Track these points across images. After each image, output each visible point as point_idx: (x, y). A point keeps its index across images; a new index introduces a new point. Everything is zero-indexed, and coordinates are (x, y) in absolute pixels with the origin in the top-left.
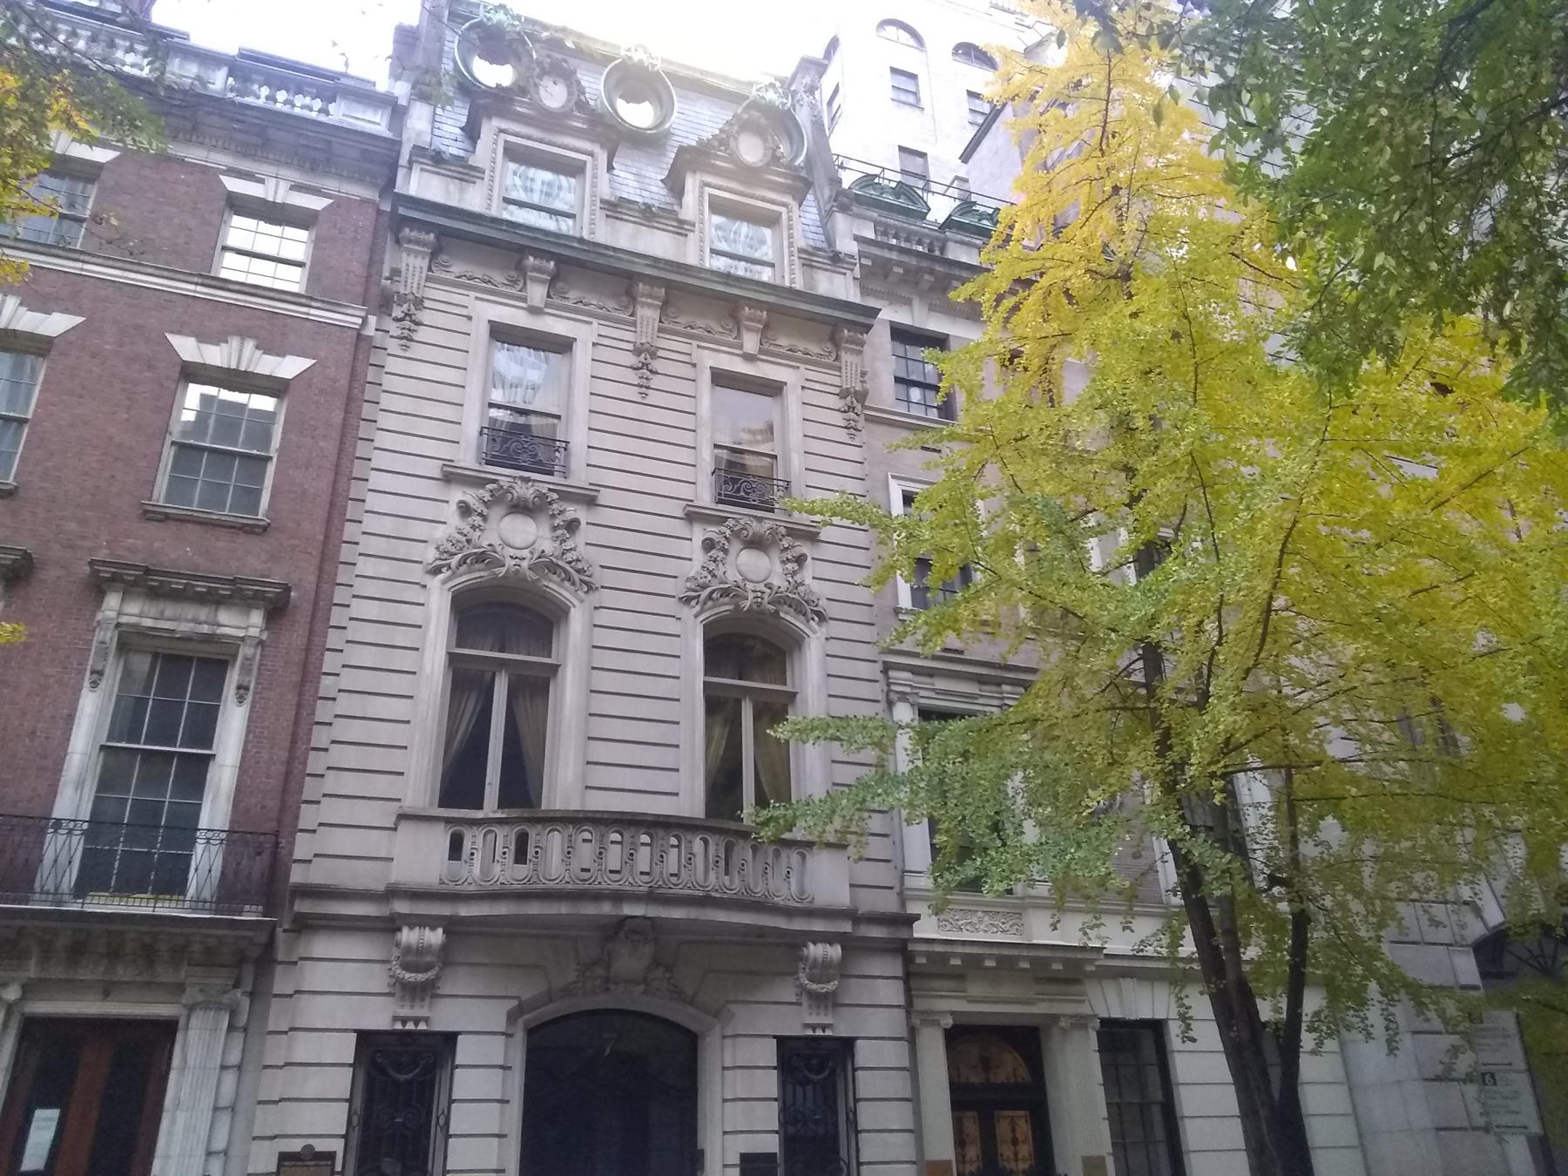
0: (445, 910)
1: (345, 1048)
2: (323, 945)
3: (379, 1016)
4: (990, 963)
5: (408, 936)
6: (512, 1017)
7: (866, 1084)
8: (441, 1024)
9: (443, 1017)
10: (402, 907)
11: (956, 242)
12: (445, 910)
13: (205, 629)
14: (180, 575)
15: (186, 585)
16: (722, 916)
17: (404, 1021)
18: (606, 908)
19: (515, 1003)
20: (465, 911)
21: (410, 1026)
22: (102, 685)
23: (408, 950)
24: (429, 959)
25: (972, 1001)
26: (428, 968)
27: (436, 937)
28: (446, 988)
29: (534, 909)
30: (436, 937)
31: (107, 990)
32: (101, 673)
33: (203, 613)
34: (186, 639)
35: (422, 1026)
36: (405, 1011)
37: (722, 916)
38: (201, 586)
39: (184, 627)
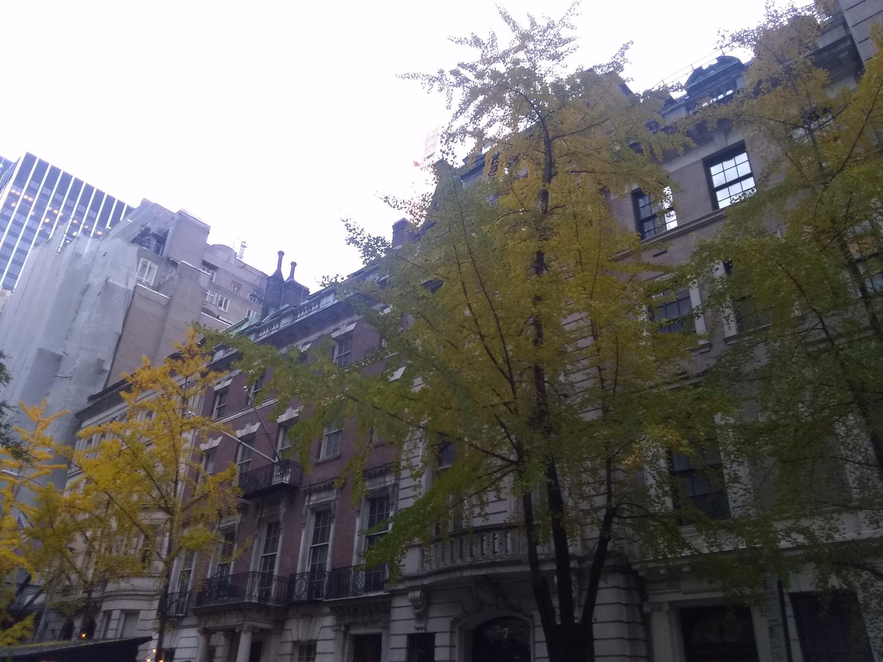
0: (418, 583)
1: (402, 642)
2: (398, 602)
3: (411, 628)
4: (686, 569)
5: (411, 595)
6: (453, 624)
7: (599, 648)
8: (430, 630)
9: (433, 626)
10: (408, 584)
11: (668, 113)
12: (418, 583)
13: (383, 485)
14: (371, 469)
15: (375, 472)
16: (503, 570)
17: (418, 629)
18: (458, 574)
19: (451, 619)
20: (426, 582)
21: (419, 631)
22: (361, 515)
23: (412, 600)
24: (420, 603)
25: (685, 593)
26: (421, 606)
27: (418, 594)
28: (432, 614)
29: (440, 578)
30: (418, 594)
31: (366, 624)
32: (359, 512)
33: (381, 479)
34: (380, 491)
35: (423, 631)
36: (418, 626)
37: (503, 570)
38: (378, 471)
39: (378, 487)
